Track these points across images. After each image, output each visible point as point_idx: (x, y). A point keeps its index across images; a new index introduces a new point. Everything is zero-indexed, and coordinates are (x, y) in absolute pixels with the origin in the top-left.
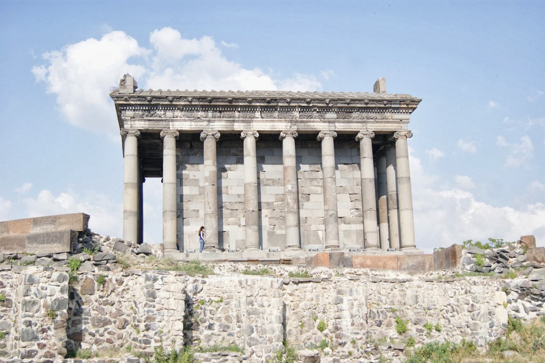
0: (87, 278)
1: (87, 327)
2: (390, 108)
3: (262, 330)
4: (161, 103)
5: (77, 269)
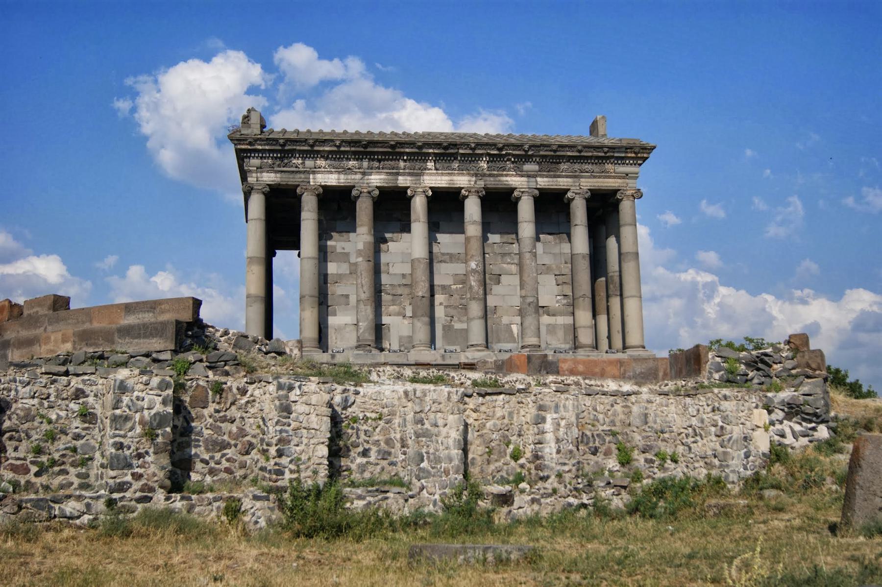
0: (198, 385)
1: (199, 451)
2: (613, 157)
3: (435, 458)
4: (298, 148)
5: (185, 373)
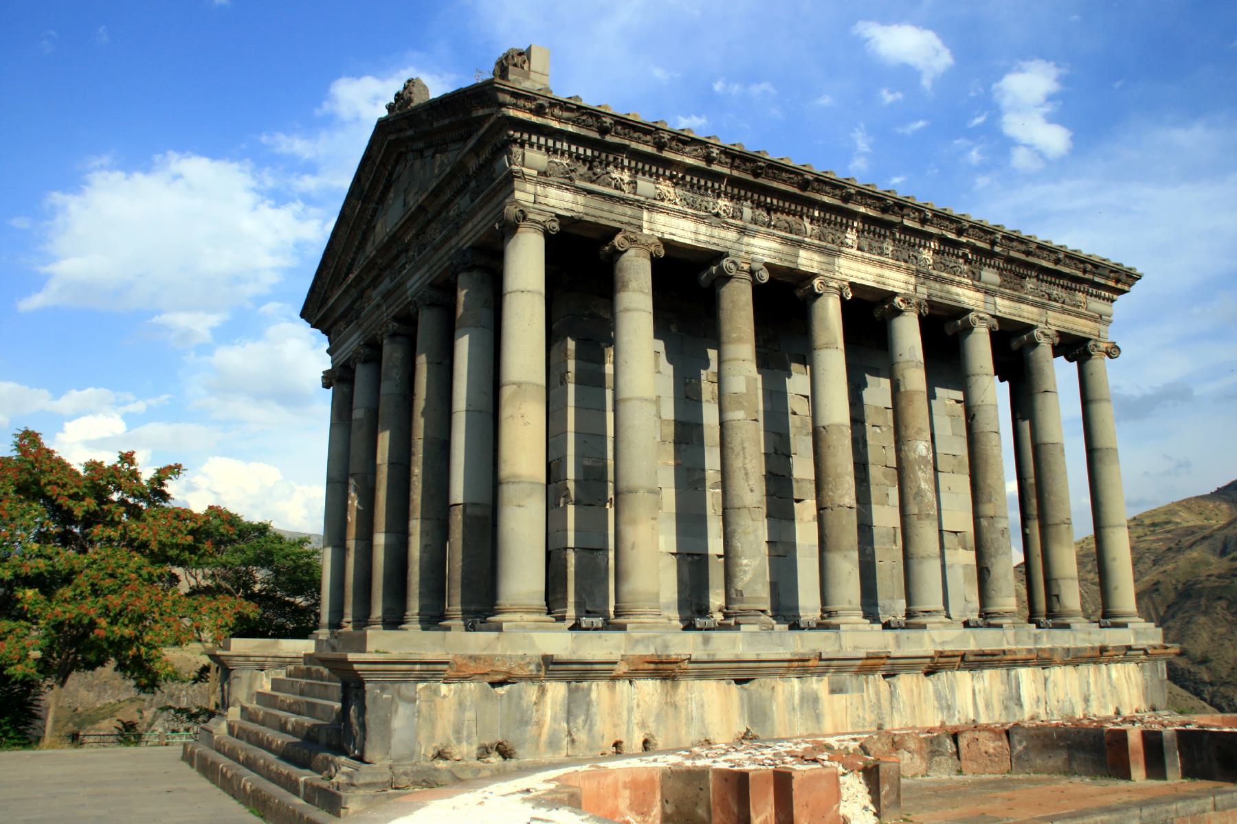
4: (634, 145)
